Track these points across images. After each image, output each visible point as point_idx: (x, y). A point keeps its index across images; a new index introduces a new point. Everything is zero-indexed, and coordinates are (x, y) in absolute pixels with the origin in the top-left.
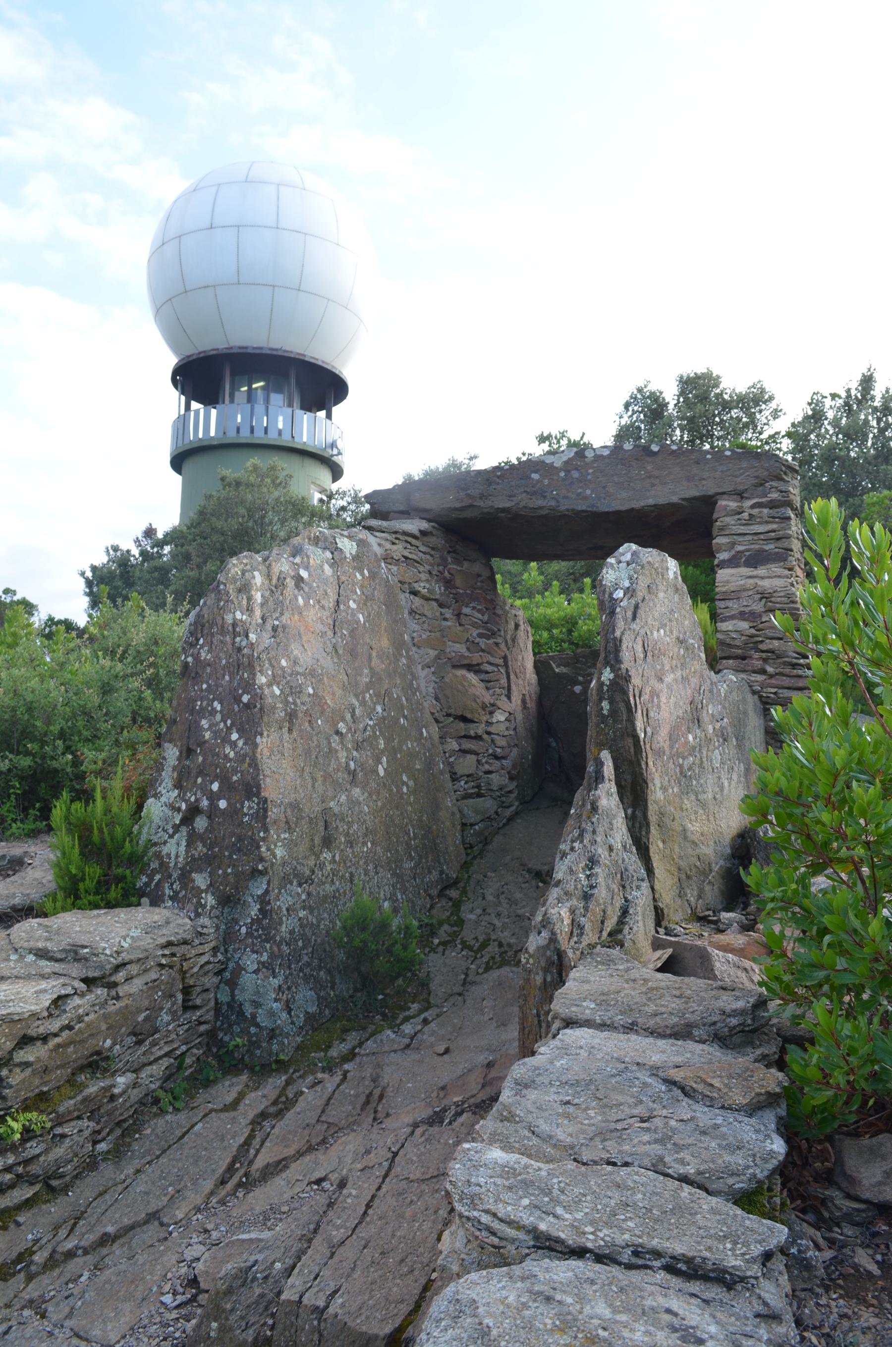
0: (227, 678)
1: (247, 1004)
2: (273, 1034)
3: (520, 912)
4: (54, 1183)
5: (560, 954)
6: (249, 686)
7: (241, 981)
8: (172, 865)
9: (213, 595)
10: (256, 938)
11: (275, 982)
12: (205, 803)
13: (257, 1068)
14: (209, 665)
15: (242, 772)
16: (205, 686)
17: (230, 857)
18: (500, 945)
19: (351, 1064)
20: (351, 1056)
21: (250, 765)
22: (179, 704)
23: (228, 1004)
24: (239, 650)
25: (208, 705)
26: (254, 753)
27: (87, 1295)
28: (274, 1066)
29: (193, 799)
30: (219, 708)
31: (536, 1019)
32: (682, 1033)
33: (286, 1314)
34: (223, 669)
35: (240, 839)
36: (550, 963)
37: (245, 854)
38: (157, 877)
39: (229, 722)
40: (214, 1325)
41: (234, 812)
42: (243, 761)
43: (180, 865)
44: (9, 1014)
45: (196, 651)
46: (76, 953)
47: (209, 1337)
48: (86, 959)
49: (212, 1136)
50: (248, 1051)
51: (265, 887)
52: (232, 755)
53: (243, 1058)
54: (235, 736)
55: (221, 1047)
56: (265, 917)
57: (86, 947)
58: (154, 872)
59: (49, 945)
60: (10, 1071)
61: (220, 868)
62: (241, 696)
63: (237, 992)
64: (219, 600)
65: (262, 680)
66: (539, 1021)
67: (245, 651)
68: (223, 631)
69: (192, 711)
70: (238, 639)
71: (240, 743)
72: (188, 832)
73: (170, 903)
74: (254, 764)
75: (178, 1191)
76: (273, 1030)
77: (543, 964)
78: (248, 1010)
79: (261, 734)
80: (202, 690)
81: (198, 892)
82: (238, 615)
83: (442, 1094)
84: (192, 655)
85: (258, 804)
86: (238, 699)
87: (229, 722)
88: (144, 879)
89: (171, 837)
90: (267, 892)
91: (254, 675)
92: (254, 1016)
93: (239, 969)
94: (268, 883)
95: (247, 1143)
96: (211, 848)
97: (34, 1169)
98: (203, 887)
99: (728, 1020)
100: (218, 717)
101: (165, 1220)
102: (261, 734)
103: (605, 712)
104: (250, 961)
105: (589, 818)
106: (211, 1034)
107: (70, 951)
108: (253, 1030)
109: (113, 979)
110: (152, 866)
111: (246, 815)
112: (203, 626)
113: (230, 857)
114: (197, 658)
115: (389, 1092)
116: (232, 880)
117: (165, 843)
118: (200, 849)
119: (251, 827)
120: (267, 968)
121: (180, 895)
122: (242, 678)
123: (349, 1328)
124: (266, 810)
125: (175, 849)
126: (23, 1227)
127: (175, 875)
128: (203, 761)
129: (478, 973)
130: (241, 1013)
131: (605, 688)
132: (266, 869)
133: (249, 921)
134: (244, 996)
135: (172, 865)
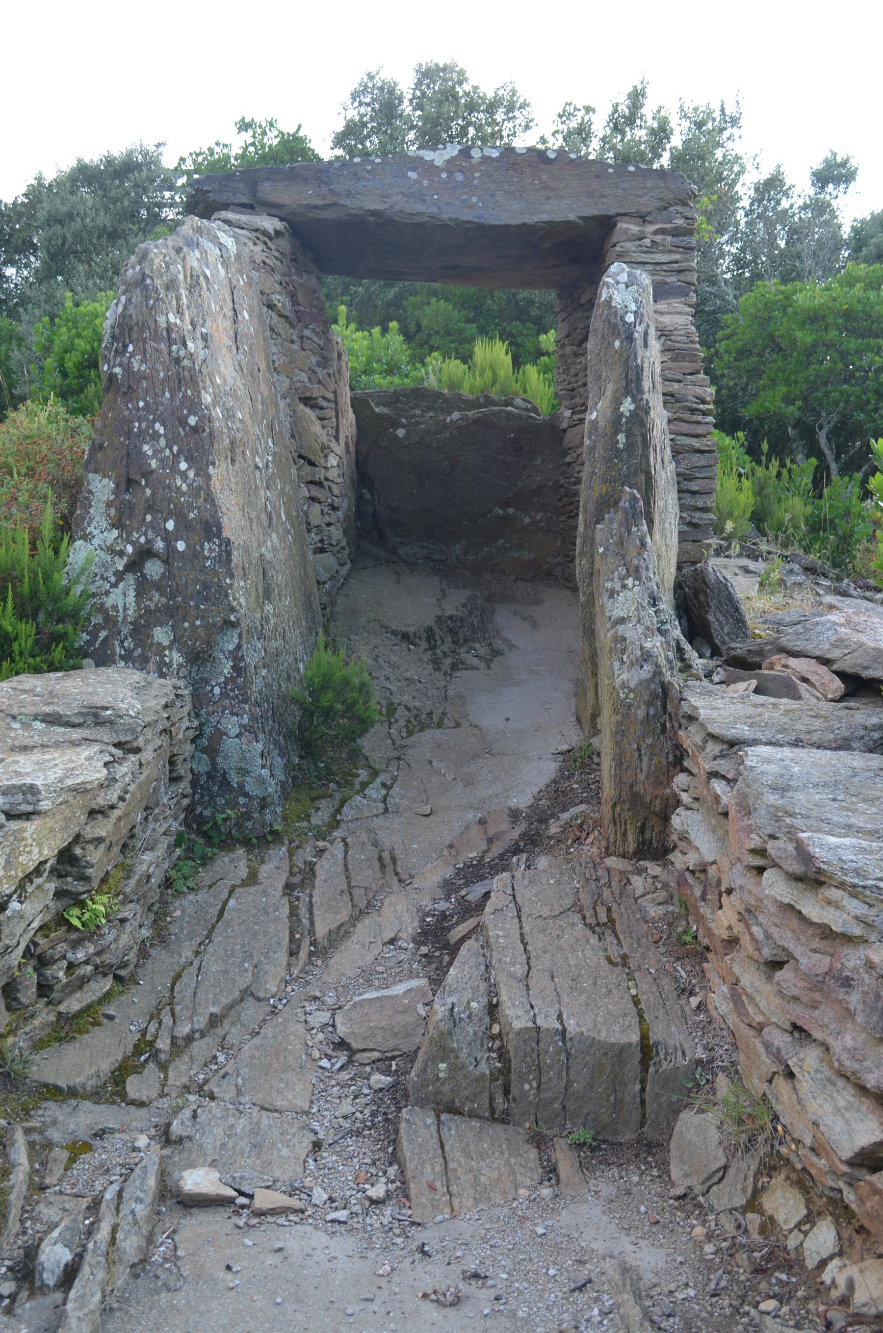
0: (167, 395)
1: (232, 772)
2: (264, 803)
3: (408, 675)
4: (123, 973)
5: (665, 688)
6: (194, 405)
7: (223, 747)
8: (120, 619)
9: (138, 291)
10: (233, 698)
11: (260, 746)
12: (160, 544)
13: (254, 841)
14: (145, 378)
15: (199, 508)
16: (141, 404)
17: (197, 607)
18: (408, 709)
19: (340, 830)
20: (335, 824)
21: (206, 500)
22: (105, 426)
23: (208, 774)
24: (178, 361)
25: (148, 427)
26: (208, 486)
27: (242, 1072)
28: (269, 838)
29: (142, 540)
30: (162, 431)
31: (636, 755)
32: (843, 745)
33: (525, 1041)
34: (162, 384)
35: (206, 586)
36: (654, 696)
37: (214, 604)
38: (103, 634)
39: (175, 448)
40: (443, 1066)
41: (194, 556)
42: (198, 495)
43: (129, 619)
44: (83, 783)
45: (125, 361)
46: (96, 716)
47: (438, 1078)
48: (111, 722)
49: (254, 911)
50: (235, 825)
51: (236, 641)
52: (184, 488)
53: (230, 833)
54: (183, 466)
55: (211, 821)
56: (239, 676)
57: (107, 708)
58: (98, 628)
59: (60, 710)
60: (83, 849)
61: (185, 620)
62: (187, 417)
63: (219, 760)
64: (147, 298)
65: (207, 399)
66: (640, 755)
67: (186, 363)
68: (156, 335)
69: (129, 434)
70: (174, 348)
71: (191, 474)
72: (137, 580)
73: (123, 663)
74: (210, 498)
75: (256, 967)
76: (264, 799)
77: (646, 698)
78: (234, 779)
79: (214, 464)
80: (138, 409)
81: (161, 649)
82: (172, 318)
83: (453, 852)
84: (121, 365)
85: (220, 546)
86: (183, 422)
87: (175, 448)
88: (85, 637)
89: (115, 586)
90: (239, 647)
91: (199, 392)
92: (241, 786)
93: (219, 734)
94: (240, 636)
95: (294, 913)
96: (172, 596)
97: (108, 958)
98: (166, 643)
99: (872, 734)
100: (163, 442)
101: (261, 995)
102: (214, 464)
103: (621, 446)
104: (231, 725)
105: (639, 554)
106: (190, 809)
107: (87, 714)
108: (242, 800)
109: (135, 744)
110: (94, 621)
111: (207, 558)
112: (131, 329)
113: (197, 607)
114: (127, 368)
115: (398, 853)
116: (203, 634)
117: (107, 593)
118: (156, 598)
119: (216, 573)
120: (249, 732)
121: (136, 654)
122: (185, 396)
123: (599, 1042)
124: (229, 553)
125: (123, 599)
126: (116, 1020)
127: (125, 631)
128: (153, 494)
129: (403, 738)
130: (225, 783)
131: (624, 420)
132: (238, 620)
133: (222, 680)
134: (229, 762)
135: (120, 619)
